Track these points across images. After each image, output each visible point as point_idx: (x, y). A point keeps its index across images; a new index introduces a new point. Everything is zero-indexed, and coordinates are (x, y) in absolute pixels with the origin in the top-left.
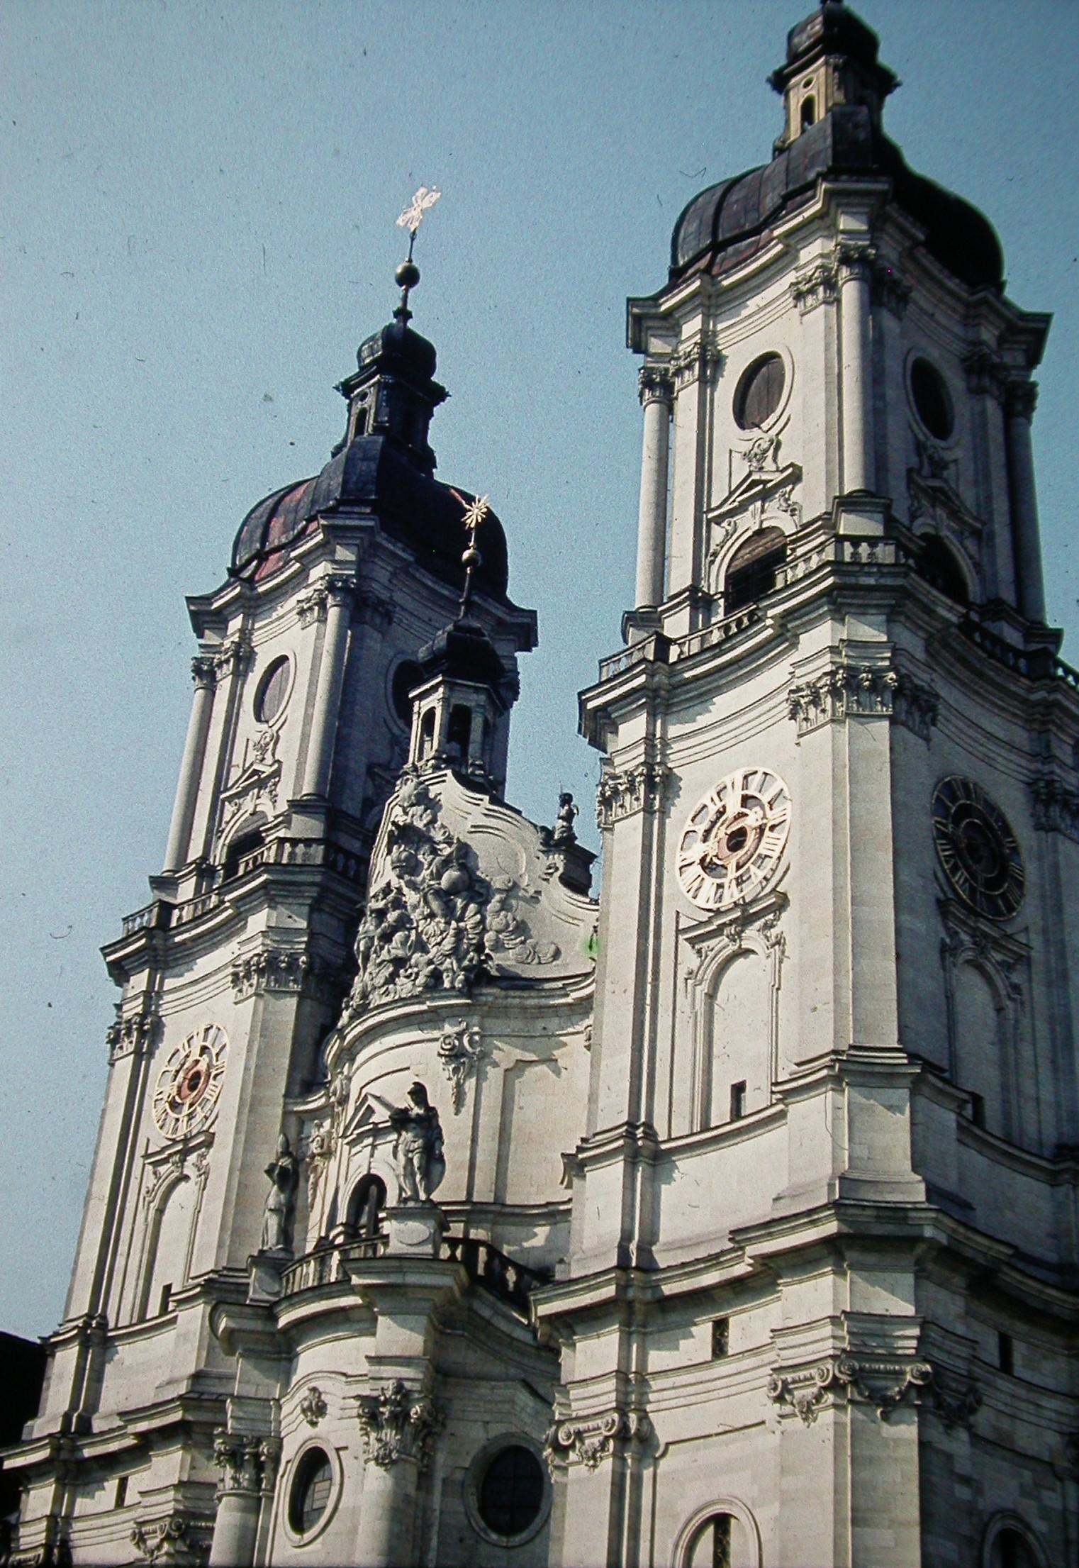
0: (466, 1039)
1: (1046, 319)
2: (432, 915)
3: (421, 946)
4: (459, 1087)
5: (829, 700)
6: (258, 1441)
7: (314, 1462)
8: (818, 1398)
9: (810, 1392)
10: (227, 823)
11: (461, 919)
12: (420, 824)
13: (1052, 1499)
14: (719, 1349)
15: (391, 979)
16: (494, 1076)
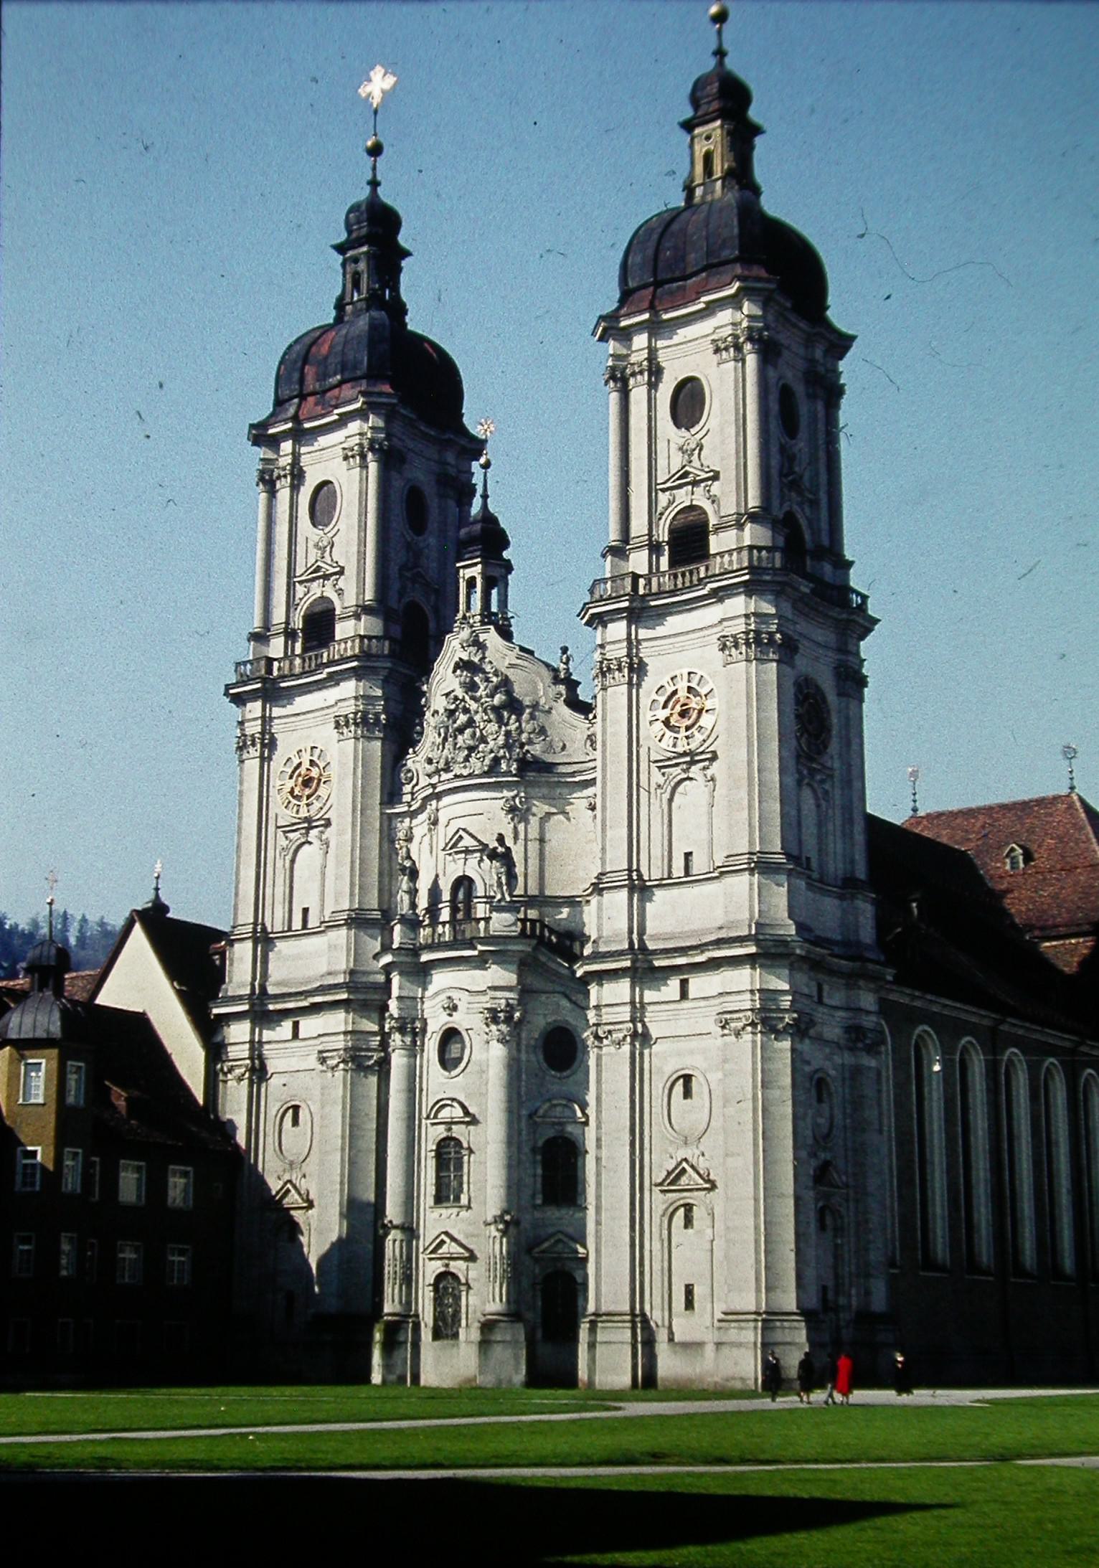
0: (517, 801)
1: (851, 339)
2: (490, 721)
3: (483, 740)
4: (515, 828)
5: (744, 647)
6: (413, 1022)
7: (450, 1036)
8: (743, 1028)
9: (740, 1025)
10: (301, 599)
11: (507, 724)
12: (476, 660)
13: (838, 1060)
14: (684, 995)
15: (467, 759)
16: (534, 821)
